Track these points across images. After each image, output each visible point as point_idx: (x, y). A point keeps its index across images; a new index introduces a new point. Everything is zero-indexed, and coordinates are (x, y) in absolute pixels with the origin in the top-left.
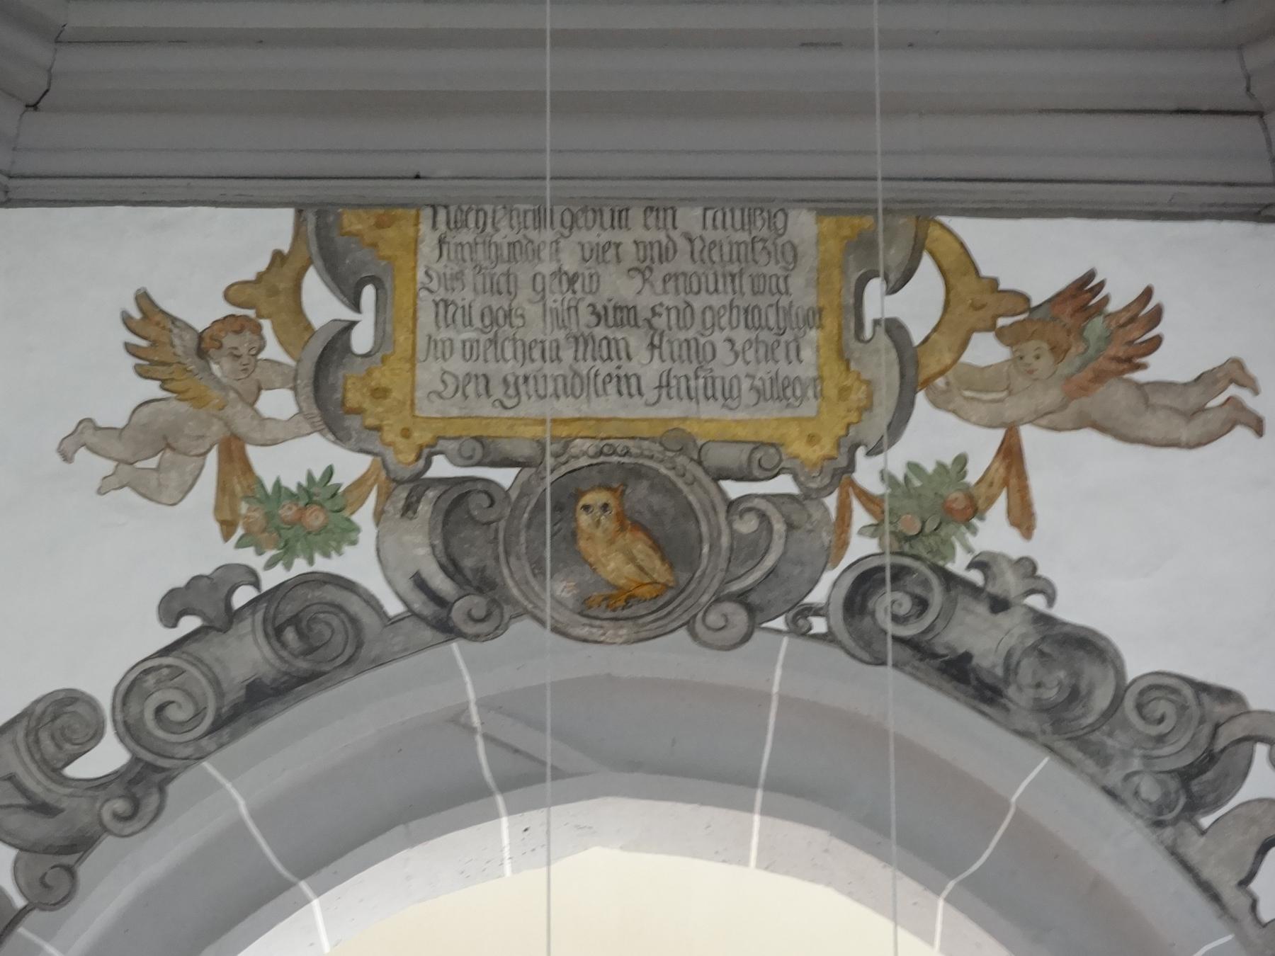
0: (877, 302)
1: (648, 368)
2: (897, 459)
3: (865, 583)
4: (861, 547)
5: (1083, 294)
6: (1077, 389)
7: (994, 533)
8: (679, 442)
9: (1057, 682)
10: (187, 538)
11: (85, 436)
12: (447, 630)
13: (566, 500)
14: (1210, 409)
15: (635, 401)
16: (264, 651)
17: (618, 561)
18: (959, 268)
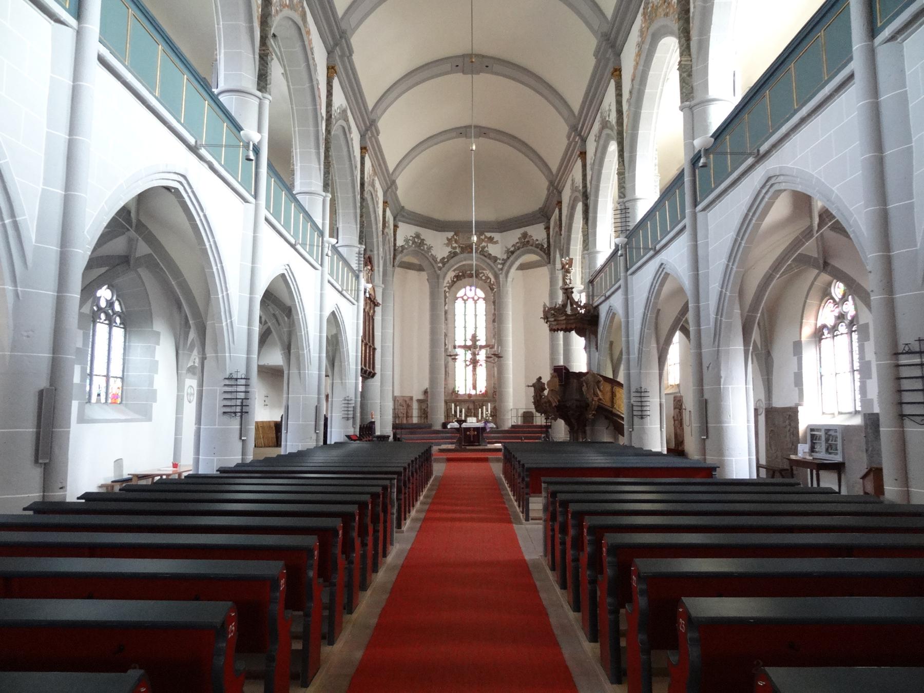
9: (489, 256)
10: (449, 249)
14: (496, 242)
16: (453, 255)
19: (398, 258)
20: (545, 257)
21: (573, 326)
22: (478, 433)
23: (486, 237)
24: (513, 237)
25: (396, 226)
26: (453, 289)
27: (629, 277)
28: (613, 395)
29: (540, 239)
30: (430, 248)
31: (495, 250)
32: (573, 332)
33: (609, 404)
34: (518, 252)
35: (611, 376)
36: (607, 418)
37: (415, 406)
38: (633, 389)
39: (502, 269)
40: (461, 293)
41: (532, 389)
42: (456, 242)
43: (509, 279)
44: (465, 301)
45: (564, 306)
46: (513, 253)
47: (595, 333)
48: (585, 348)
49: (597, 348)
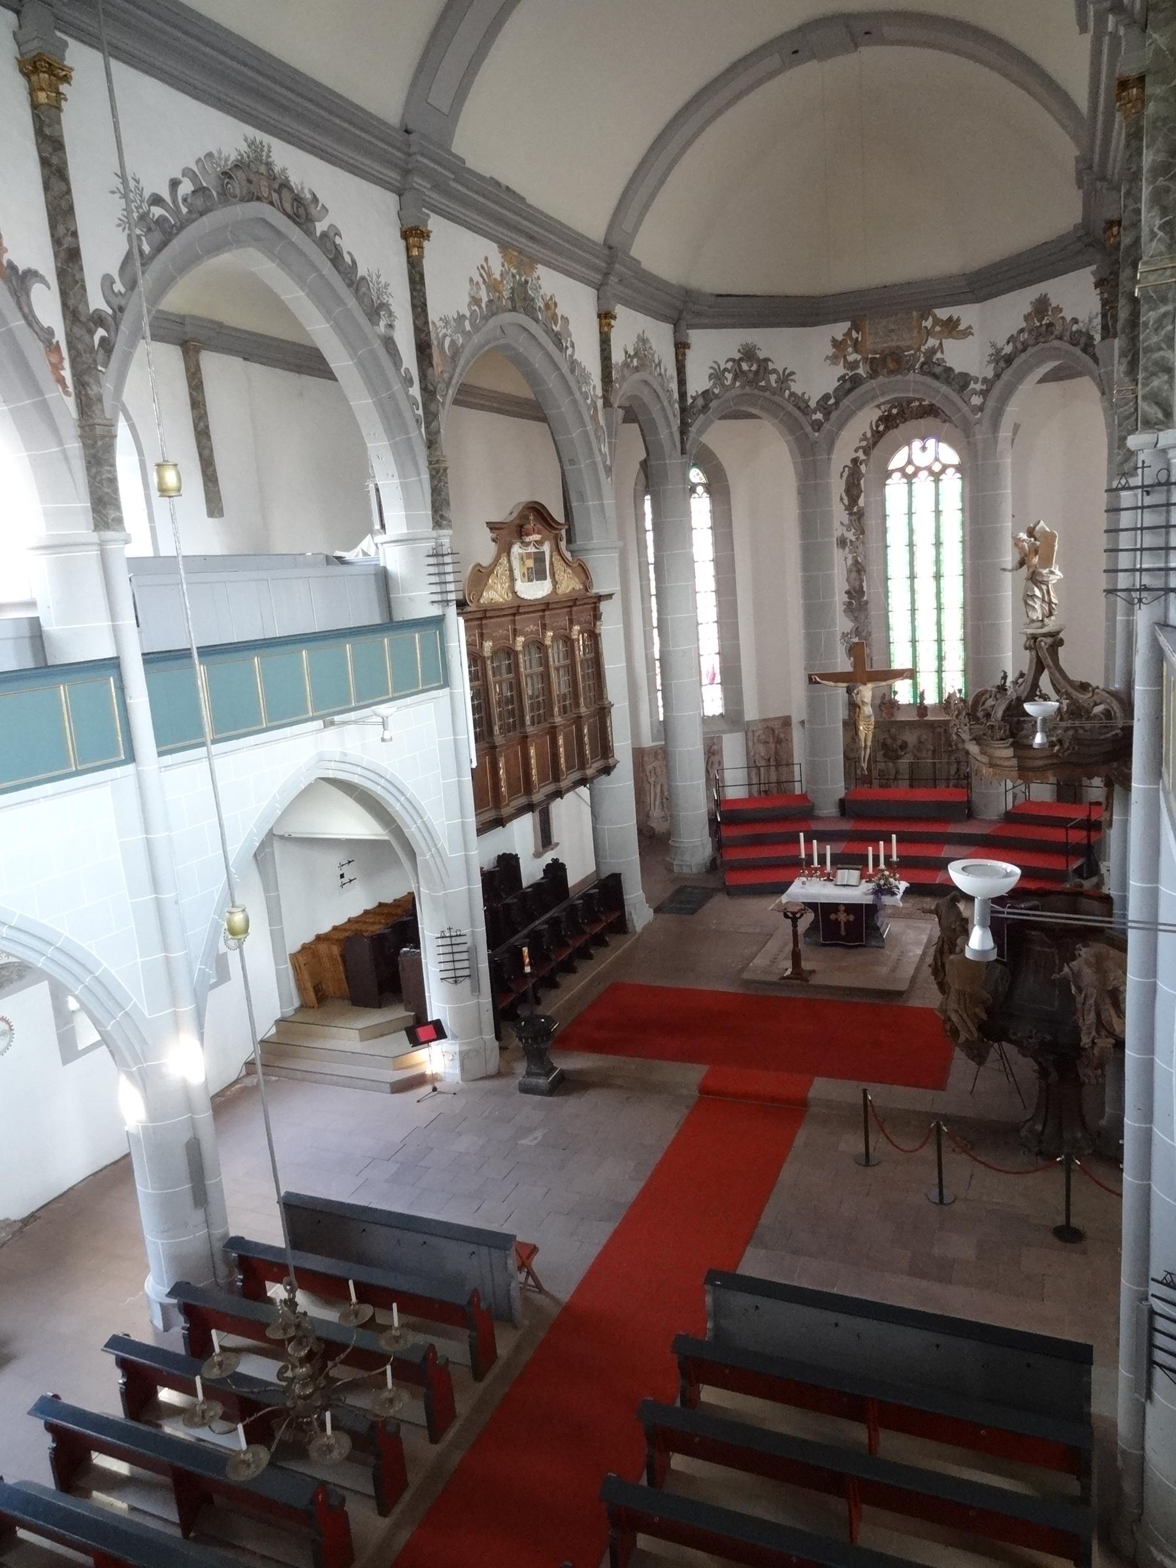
0: (924, 324)
1: (895, 338)
2: (926, 347)
3: (923, 364)
4: (922, 359)
5: (950, 319)
6: (950, 332)
7: (939, 355)
8: (898, 347)
10: (840, 370)
11: (827, 358)
12: (871, 378)
13: (884, 359)
14: (967, 332)
15: (893, 342)
16: (850, 384)
17: (891, 366)
18: (935, 317)
19: (693, 429)
22: (858, 919)
23: (937, 322)
24: (1007, 315)
25: (681, 347)
26: (875, 452)
29: (1083, 317)
30: (785, 378)
31: (965, 356)
34: (1023, 356)
37: (798, 738)
39: (981, 409)
40: (898, 460)
42: (856, 346)
43: (1005, 433)
44: (909, 478)
46: (1009, 360)
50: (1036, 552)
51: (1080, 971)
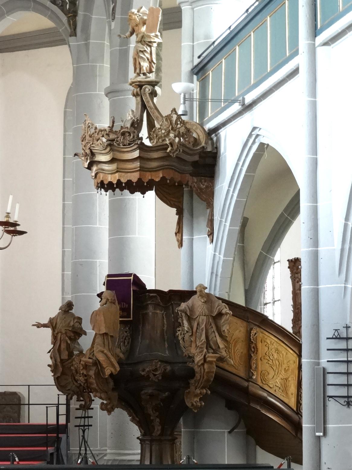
20: (64, 19)
21: (158, 177)
27: (321, 51)
28: (251, 348)
32: (151, 194)
33: (242, 372)
35: (240, 301)
36: (231, 405)
38: (326, 331)
41: (48, 332)
45: (136, 125)
47: (208, 197)
48: (179, 231)
49: (211, 234)
50: (144, 23)
51: (193, 306)
